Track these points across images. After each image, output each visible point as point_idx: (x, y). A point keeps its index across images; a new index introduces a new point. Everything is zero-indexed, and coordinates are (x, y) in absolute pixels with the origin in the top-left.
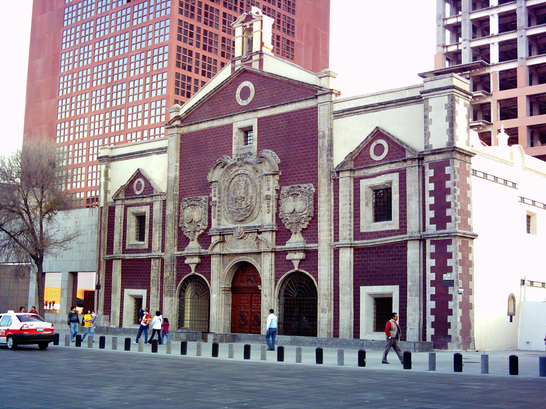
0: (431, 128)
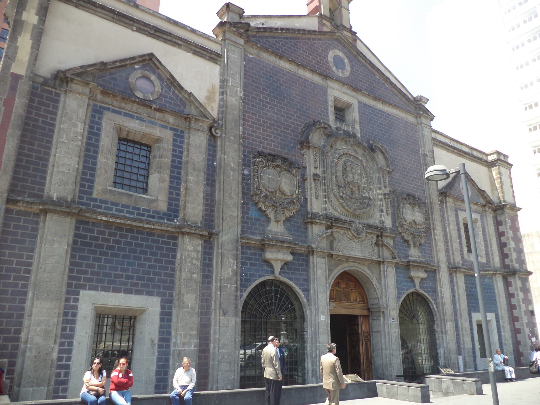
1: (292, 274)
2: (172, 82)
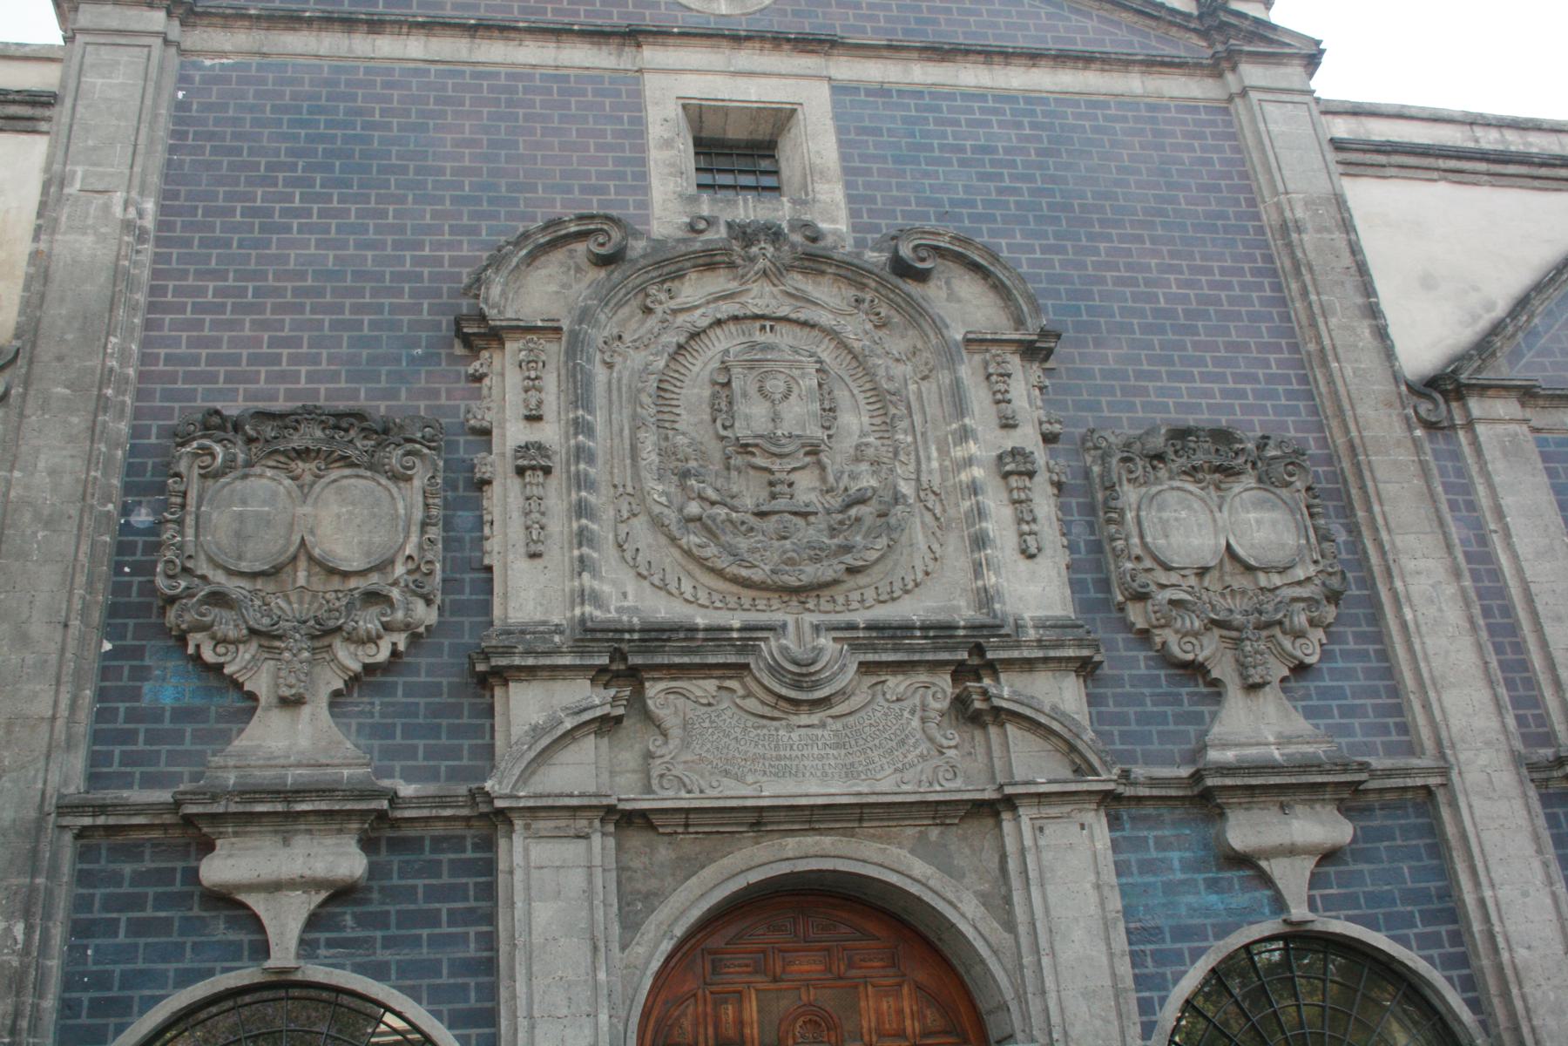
1: (388, 943)
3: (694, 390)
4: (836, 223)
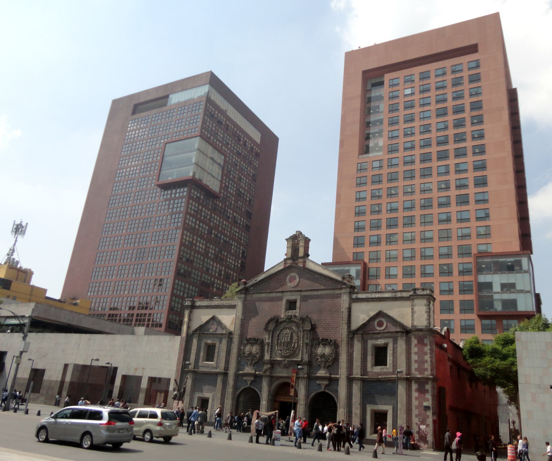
0: (415, 315)
2: (220, 323)
3: (281, 336)
4: (297, 315)
